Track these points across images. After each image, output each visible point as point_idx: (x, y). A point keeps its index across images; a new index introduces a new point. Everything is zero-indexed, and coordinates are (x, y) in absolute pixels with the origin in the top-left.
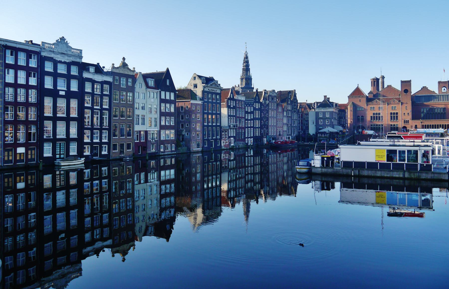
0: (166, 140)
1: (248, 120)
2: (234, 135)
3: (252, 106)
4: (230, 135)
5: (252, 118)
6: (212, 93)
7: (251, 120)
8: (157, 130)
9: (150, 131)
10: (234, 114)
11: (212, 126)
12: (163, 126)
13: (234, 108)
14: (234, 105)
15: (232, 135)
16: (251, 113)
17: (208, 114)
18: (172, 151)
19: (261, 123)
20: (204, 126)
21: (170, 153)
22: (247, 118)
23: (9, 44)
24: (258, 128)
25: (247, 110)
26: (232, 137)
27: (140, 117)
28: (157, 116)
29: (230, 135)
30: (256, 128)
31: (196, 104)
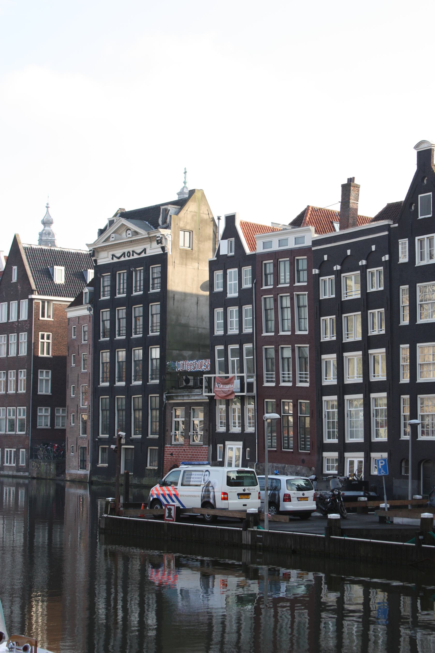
0: (6, 436)
1: (340, 347)
2: (250, 429)
5: (378, 329)
6: (129, 266)
7: (367, 343)
10: (248, 330)
11: (128, 391)
13: (245, 297)
14: (247, 285)
15: (236, 430)
16: (366, 302)
17: (113, 346)
18: (18, 469)
20: (97, 392)
21: (15, 473)
22: (327, 336)
25: (327, 293)
26: (234, 437)
29: (221, 429)
31: (79, 317)
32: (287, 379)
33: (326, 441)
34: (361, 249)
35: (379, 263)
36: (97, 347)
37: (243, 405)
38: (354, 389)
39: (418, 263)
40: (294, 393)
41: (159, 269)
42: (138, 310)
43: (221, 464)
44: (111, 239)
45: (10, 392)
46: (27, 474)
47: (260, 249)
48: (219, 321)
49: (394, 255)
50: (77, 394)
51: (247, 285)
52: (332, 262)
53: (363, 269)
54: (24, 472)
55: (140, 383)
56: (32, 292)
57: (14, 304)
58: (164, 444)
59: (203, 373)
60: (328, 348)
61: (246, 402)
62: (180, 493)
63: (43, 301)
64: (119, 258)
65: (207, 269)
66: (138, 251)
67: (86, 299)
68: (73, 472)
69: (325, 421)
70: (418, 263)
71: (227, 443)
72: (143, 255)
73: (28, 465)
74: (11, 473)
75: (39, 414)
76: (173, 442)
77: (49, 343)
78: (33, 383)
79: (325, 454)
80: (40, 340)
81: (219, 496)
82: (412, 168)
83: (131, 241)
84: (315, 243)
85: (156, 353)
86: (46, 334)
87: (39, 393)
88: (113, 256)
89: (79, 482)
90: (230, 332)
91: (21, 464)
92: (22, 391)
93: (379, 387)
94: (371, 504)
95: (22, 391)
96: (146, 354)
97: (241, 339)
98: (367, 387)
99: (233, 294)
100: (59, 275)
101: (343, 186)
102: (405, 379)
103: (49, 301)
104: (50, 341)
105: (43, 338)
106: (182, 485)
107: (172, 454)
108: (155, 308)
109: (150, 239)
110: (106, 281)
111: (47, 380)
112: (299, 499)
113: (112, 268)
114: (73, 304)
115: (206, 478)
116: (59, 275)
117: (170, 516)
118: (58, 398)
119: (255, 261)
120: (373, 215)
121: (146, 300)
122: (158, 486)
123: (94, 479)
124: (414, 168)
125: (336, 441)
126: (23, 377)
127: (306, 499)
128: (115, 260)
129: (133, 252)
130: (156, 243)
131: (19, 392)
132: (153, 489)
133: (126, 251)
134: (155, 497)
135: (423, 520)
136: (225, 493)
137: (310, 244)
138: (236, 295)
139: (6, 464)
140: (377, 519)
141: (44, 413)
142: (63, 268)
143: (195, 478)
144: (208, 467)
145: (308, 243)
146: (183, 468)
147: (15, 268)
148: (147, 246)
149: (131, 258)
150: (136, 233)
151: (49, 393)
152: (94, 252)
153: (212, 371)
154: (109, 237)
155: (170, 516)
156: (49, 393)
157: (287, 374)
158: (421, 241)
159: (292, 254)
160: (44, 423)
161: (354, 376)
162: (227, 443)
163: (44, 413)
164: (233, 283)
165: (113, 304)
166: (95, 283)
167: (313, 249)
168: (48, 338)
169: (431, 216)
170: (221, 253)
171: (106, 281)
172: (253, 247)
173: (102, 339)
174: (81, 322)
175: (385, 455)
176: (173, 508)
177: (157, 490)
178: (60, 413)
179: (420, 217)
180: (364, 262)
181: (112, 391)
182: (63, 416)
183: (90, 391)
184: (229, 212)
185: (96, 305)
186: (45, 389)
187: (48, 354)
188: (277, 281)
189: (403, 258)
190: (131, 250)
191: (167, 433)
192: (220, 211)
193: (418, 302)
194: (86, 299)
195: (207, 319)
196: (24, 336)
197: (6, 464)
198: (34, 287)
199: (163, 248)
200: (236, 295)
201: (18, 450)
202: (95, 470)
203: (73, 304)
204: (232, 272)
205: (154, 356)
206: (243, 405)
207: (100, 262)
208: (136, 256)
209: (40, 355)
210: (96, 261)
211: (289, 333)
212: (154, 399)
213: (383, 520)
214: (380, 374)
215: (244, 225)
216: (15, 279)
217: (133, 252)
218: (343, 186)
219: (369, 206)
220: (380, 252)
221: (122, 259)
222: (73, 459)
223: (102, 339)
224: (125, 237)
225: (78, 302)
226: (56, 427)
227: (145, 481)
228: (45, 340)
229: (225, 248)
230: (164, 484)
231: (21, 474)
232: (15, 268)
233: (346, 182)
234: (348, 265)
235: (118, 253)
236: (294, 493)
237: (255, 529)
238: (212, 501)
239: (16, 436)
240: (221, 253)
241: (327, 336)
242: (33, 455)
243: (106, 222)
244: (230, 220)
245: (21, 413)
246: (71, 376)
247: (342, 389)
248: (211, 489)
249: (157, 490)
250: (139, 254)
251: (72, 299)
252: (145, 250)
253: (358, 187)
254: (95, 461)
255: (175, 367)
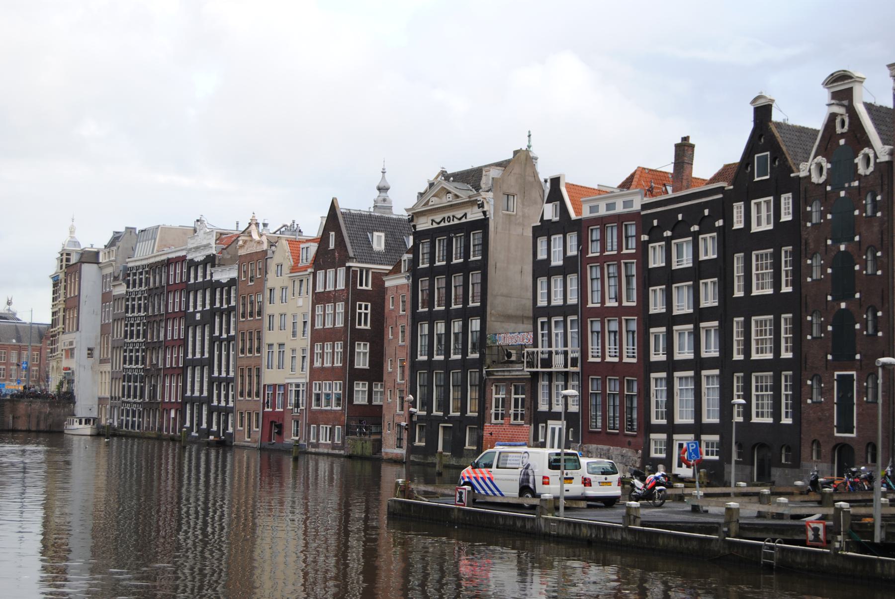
1: (669, 320)
3: (707, 228)
4: (543, 407)
5: (709, 299)
7: (699, 315)
8: (303, 381)
9: (291, 384)
10: (573, 300)
11: (447, 365)
12: (318, 368)
13: (570, 266)
14: (572, 252)
16: (699, 271)
17: (432, 317)
18: (334, 447)
19: (799, 329)
20: (415, 366)
21: (330, 451)
22: (657, 307)
23: (170, 256)
24: (776, 365)
25: (656, 260)
26: (556, 416)
27: (276, 349)
28: (306, 342)
29: (543, 407)
30: (750, 366)
32: (596, 354)
33: (654, 421)
34: (694, 214)
35: (712, 229)
36: (416, 319)
37: (550, 381)
38: (684, 365)
39: (755, 229)
40: (618, 369)
41: (480, 235)
42: (457, 280)
43: (543, 445)
44: (430, 203)
45: (325, 365)
46: (342, 452)
47: (586, 214)
48: (542, 290)
49: (729, 221)
50: (395, 368)
51: (572, 252)
52: (661, 228)
53: (695, 235)
54: (340, 450)
55: (459, 357)
56: (350, 259)
57: (331, 273)
58: (484, 422)
59: (526, 346)
60: (657, 320)
61: (554, 379)
62: (494, 476)
63: (361, 269)
64: (439, 223)
65: (529, 233)
66: (459, 216)
67: (404, 267)
68: (389, 450)
69: (653, 400)
70: (755, 229)
71: (549, 422)
72: (464, 220)
73: (343, 443)
74: (326, 451)
75: (355, 389)
76: (493, 421)
77: (366, 314)
78: (349, 356)
79: (653, 436)
80: (358, 311)
81: (539, 480)
82: (750, 126)
83: (451, 206)
84: (645, 207)
85: (475, 325)
86: (363, 304)
87: (356, 367)
88: (433, 221)
89: (396, 461)
90: (553, 303)
91: (336, 442)
92: (338, 364)
93: (710, 363)
94: (687, 491)
95: (338, 364)
96: (465, 327)
97: (565, 310)
98: (698, 364)
99: (557, 261)
100: (379, 242)
101: (677, 146)
102: (738, 357)
103: (368, 270)
104: (369, 311)
105: (360, 308)
106: (498, 467)
107: (491, 434)
108: (475, 277)
109: (472, 203)
110: (424, 249)
111: (365, 354)
112: (601, 483)
113: (431, 235)
114: (391, 272)
115: (525, 460)
116: (379, 242)
117: (461, 500)
118: (375, 374)
119: (581, 227)
120: (708, 176)
121: (466, 268)
122: (469, 468)
123: (412, 458)
124: (751, 126)
125: (664, 422)
126: (339, 348)
127: (609, 483)
128: (435, 225)
129: (454, 216)
130: (477, 207)
131: (335, 365)
132: (464, 471)
133: (446, 215)
134: (467, 480)
135: (729, 509)
136: (544, 477)
137: (639, 208)
138: (561, 263)
139: (321, 441)
140: (689, 508)
141: (360, 389)
142: (383, 235)
143: (511, 461)
144: (525, 449)
145: (637, 207)
146: (498, 449)
147: (332, 234)
148: (468, 211)
149: (452, 223)
150: (457, 196)
151: (367, 367)
152: (415, 216)
153: (535, 345)
154: (428, 201)
155: (461, 500)
156: (367, 367)
157: (610, 348)
158: (758, 205)
159: (620, 220)
160: (360, 399)
161: (684, 353)
162: (549, 422)
163: (360, 389)
164: (558, 250)
165: (432, 272)
166: (415, 250)
167: (643, 213)
168: (366, 308)
169: (767, 177)
170: (545, 218)
171: (424, 249)
172: (578, 211)
173: (420, 310)
174: (399, 291)
175: (716, 438)
176: (463, 491)
177: (468, 472)
178: (377, 388)
179: (756, 179)
180: (695, 228)
181: (430, 365)
182: (381, 392)
183: (407, 364)
184: (554, 174)
185: (415, 274)
186: (362, 362)
187: (366, 324)
188: (603, 248)
189: (738, 225)
190: (451, 214)
191: (487, 411)
192: (545, 172)
193: (754, 271)
194: (404, 267)
195: (531, 289)
196: (340, 308)
197: (321, 441)
198: (351, 254)
199: (484, 213)
200: (561, 263)
201: (334, 426)
202: (412, 450)
203: (391, 272)
204: (557, 239)
205: (474, 329)
206: (550, 381)
207: (419, 228)
208: (456, 222)
209: (357, 327)
210: (414, 226)
211: (599, 305)
212: (472, 376)
213: (695, 509)
214: (711, 351)
215: (569, 186)
216: (332, 246)
217: (454, 216)
218: (677, 146)
219: (705, 167)
220: (713, 217)
221: (442, 224)
222: (389, 436)
223: (420, 310)
224: (446, 200)
225: (396, 270)
226: (374, 403)
227: (463, 461)
228: (363, 311)
229: (550, 212)
230: (476, 466)
231: (337, 452)
232: (332, 234)
233: (679, 141)
234: (680, 230)
235: (438, 218)
236: (595, 478)
237: (550, 516)
238: (531, 486)
239: (322, 412)
240: (545, 218)
241: (657, 307)
242: (348, 431)
243: (427, 185)
244: (555, 182)
245: (336, 388)
246: (389, 350)
247: (671, 366)
248: (530, 472)
249: (468, 472)
250: (460, 219)
251: (391, 268)
252: (465, 215)
253: (693, 146)
254: (411, 439)
255: (496, 340)
